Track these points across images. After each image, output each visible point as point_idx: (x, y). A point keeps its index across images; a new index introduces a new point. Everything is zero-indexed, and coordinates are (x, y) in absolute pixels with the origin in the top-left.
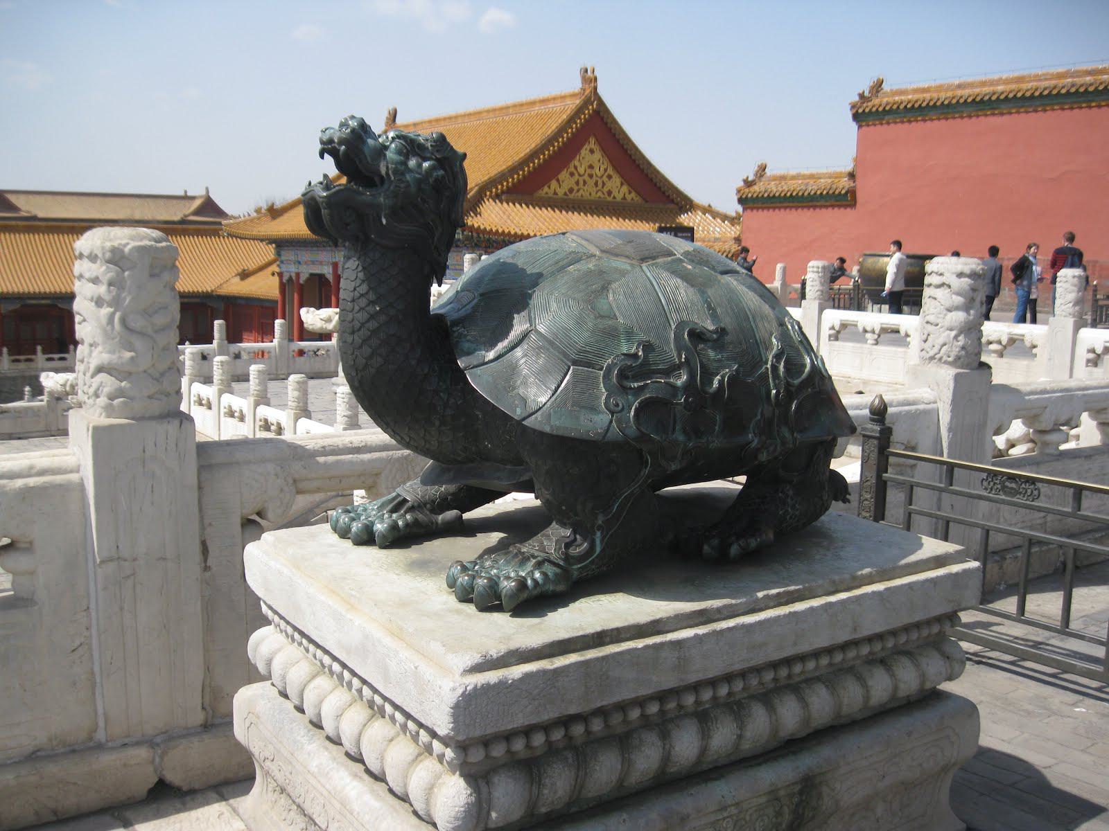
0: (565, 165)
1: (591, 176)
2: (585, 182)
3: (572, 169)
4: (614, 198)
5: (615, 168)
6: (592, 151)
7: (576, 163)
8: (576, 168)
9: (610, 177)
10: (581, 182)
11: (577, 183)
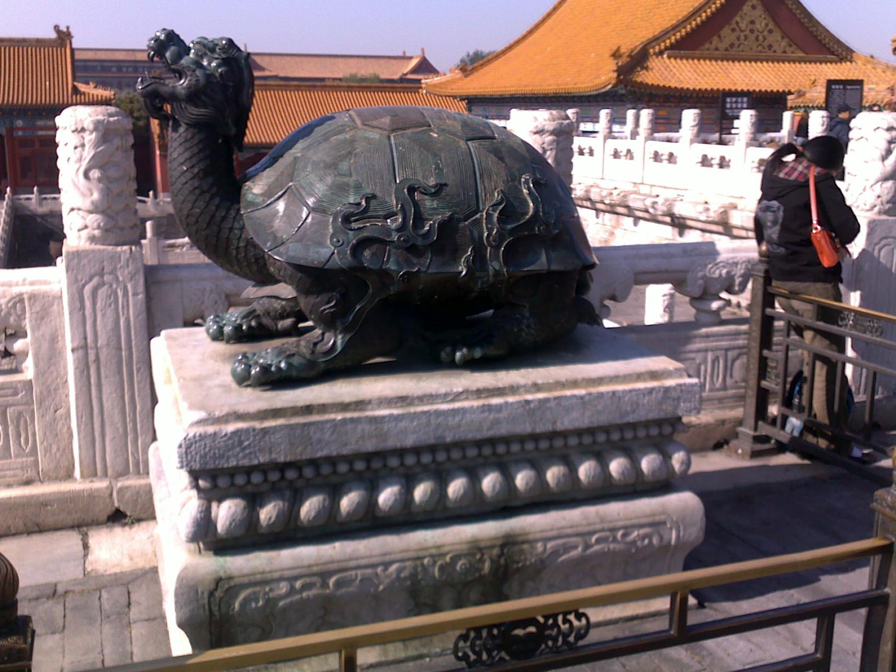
0: (727, 22)
1: (752, 31)
2: (746, 37)
3: (734, 26)
4: (775, 52)
5: (777, 23)
6: (754, 7)
7: (738, 19)
8: (737, 23)
9: (770, 31)
10: (742, 38)
11: (738, 38)
